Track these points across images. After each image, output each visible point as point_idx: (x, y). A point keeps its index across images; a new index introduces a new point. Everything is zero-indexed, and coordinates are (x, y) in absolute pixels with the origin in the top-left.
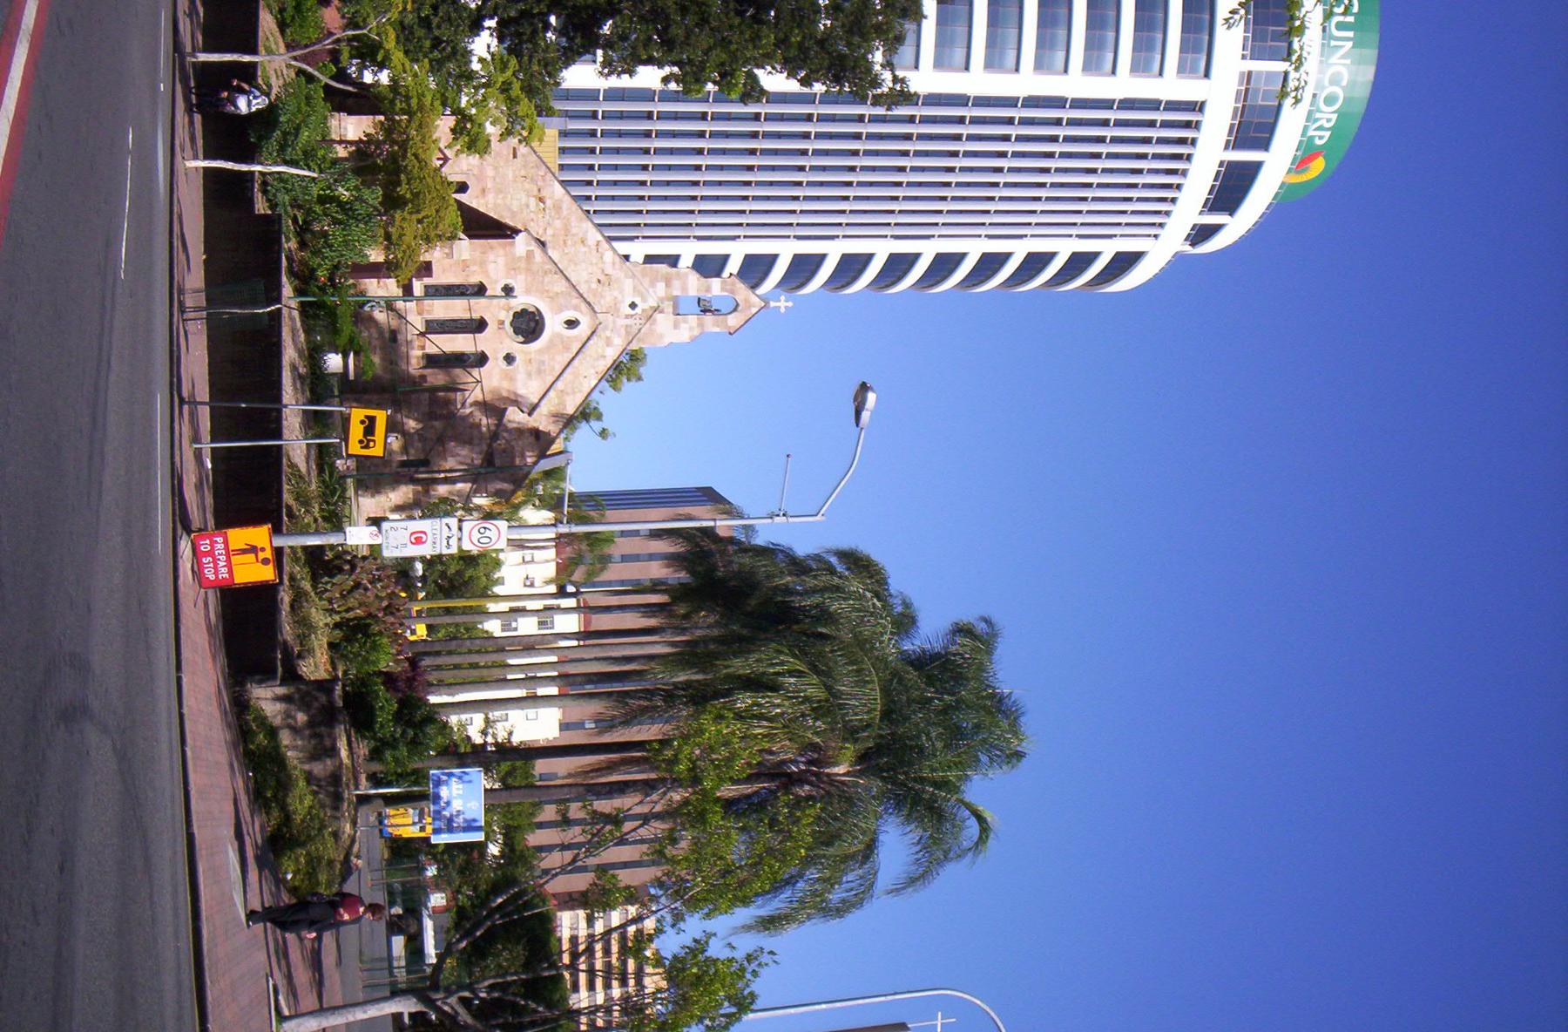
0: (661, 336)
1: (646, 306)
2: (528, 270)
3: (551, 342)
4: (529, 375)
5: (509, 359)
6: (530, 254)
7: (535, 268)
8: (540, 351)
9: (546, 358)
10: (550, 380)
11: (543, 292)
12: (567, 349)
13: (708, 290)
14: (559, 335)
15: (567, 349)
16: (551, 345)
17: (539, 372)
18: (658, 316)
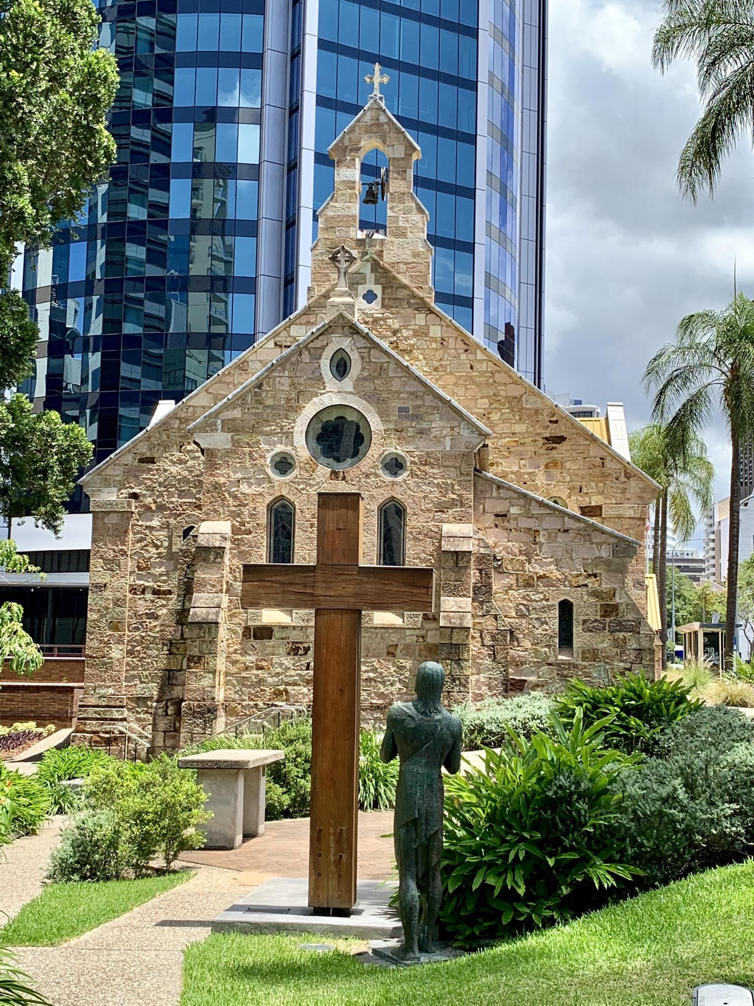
0: (416, 255)
1: (370, 277)
2: (253, 430)
3: (367, 397)
4: (421, 432)
5: (395, 465)
6: (231, 427)
7: (251, 420)
8: (383, 415)
9: (396, 404)
10: (428, 400)
11: (293, 408)
12: (382, 369)
13: (351, 185)
14: (360, 380)
15: (382, 369)
16: (372, 398)
17: (417, 417)
18: (387, 259)
